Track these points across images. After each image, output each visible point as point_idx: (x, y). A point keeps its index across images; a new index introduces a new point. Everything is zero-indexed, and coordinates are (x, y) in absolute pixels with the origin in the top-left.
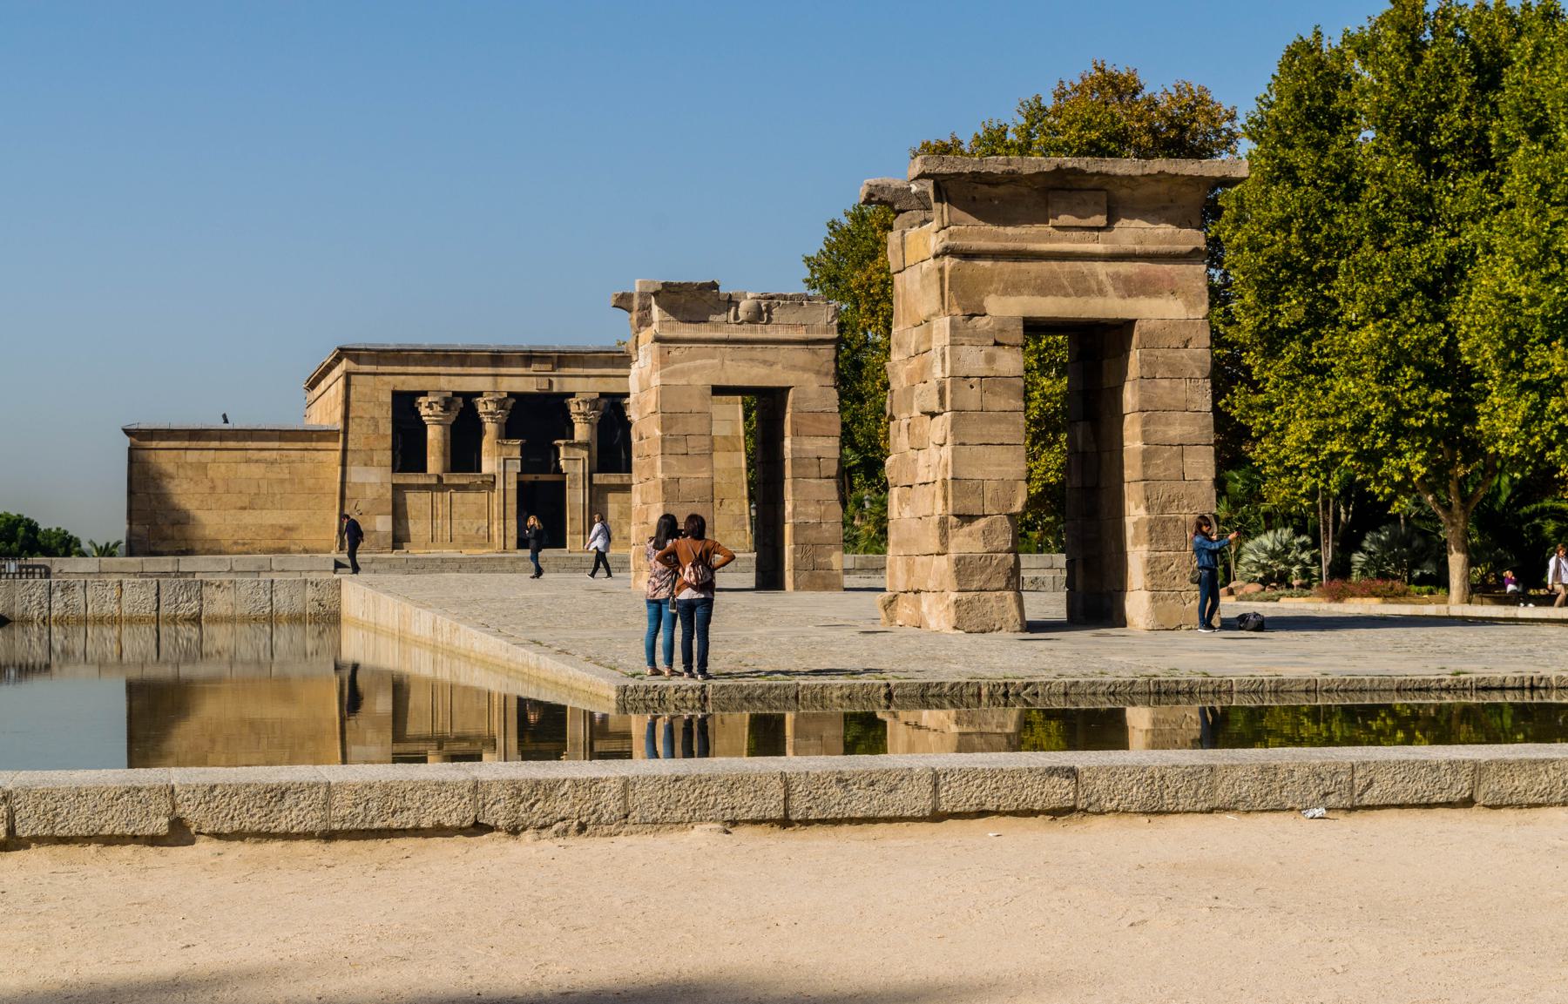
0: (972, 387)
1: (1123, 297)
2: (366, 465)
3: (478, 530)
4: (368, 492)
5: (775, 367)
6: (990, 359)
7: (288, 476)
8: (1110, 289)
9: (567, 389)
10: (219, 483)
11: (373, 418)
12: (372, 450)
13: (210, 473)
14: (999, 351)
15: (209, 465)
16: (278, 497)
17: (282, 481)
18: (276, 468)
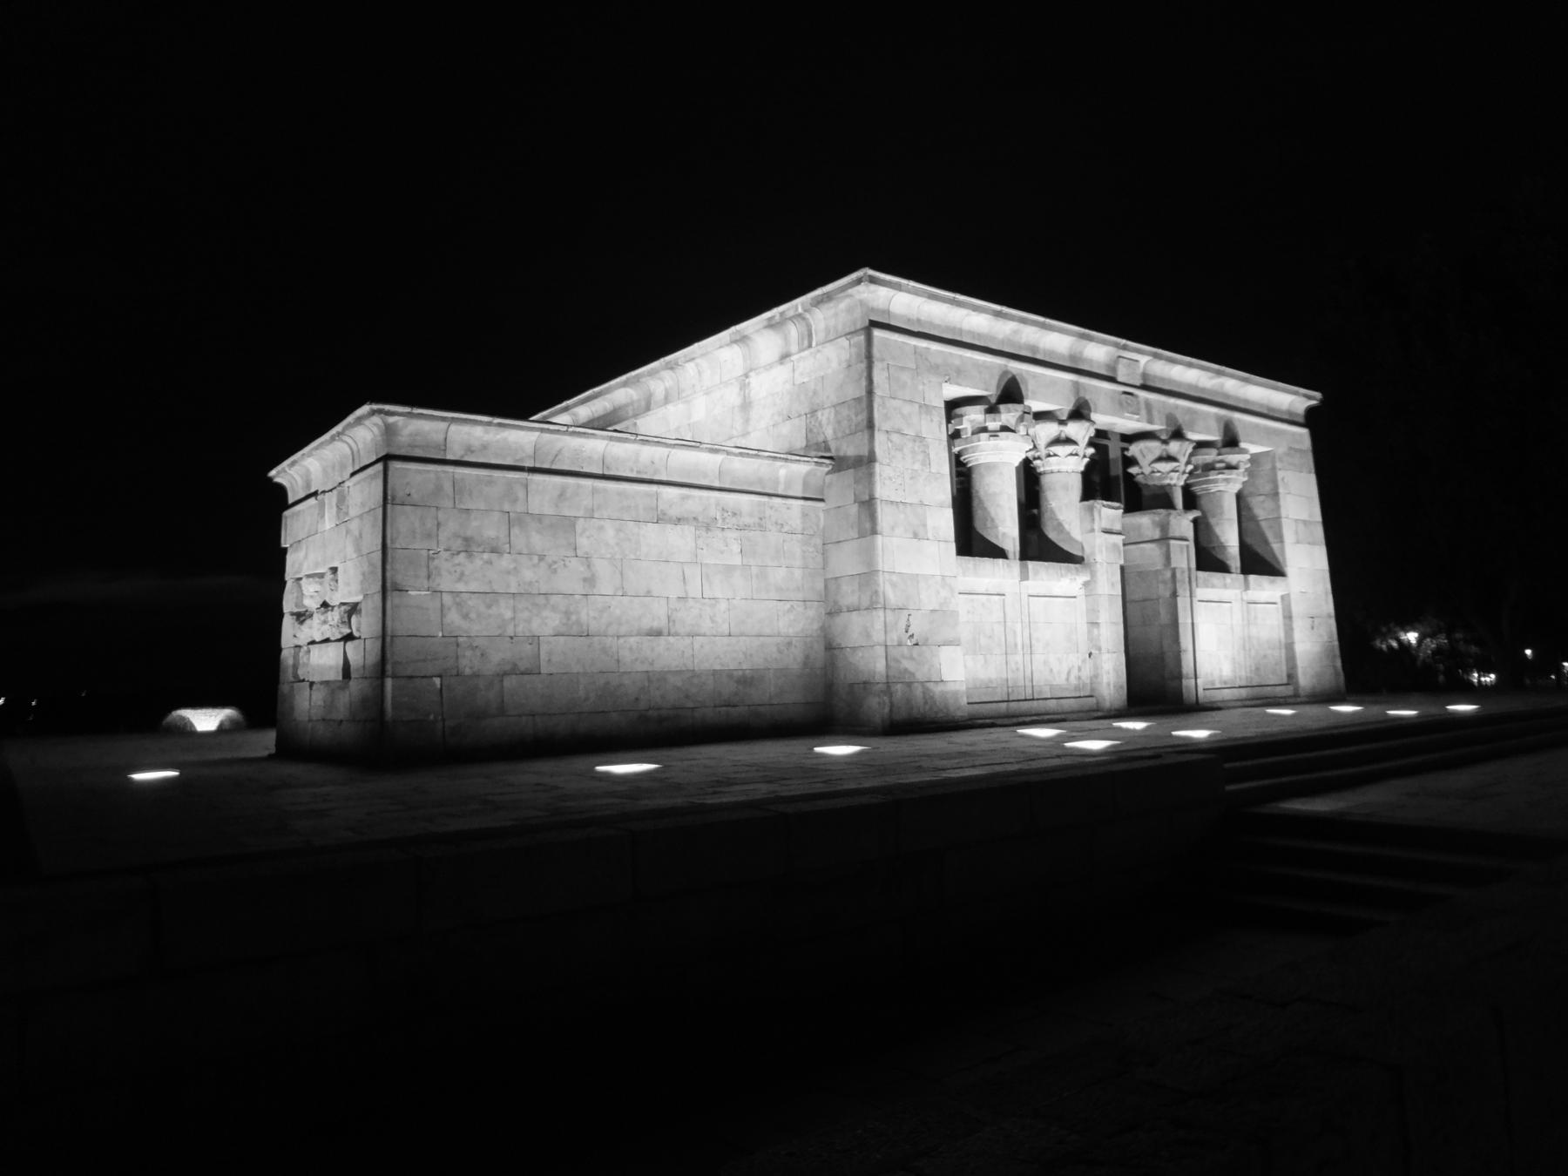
2: (916, 536)
7: (737, 560)
10: (602, 568)
11: (919, 438)
12: (922, 504)
13: (583, 543)
15: (580, 524)
16: (723, 606)
17: (729, 569)
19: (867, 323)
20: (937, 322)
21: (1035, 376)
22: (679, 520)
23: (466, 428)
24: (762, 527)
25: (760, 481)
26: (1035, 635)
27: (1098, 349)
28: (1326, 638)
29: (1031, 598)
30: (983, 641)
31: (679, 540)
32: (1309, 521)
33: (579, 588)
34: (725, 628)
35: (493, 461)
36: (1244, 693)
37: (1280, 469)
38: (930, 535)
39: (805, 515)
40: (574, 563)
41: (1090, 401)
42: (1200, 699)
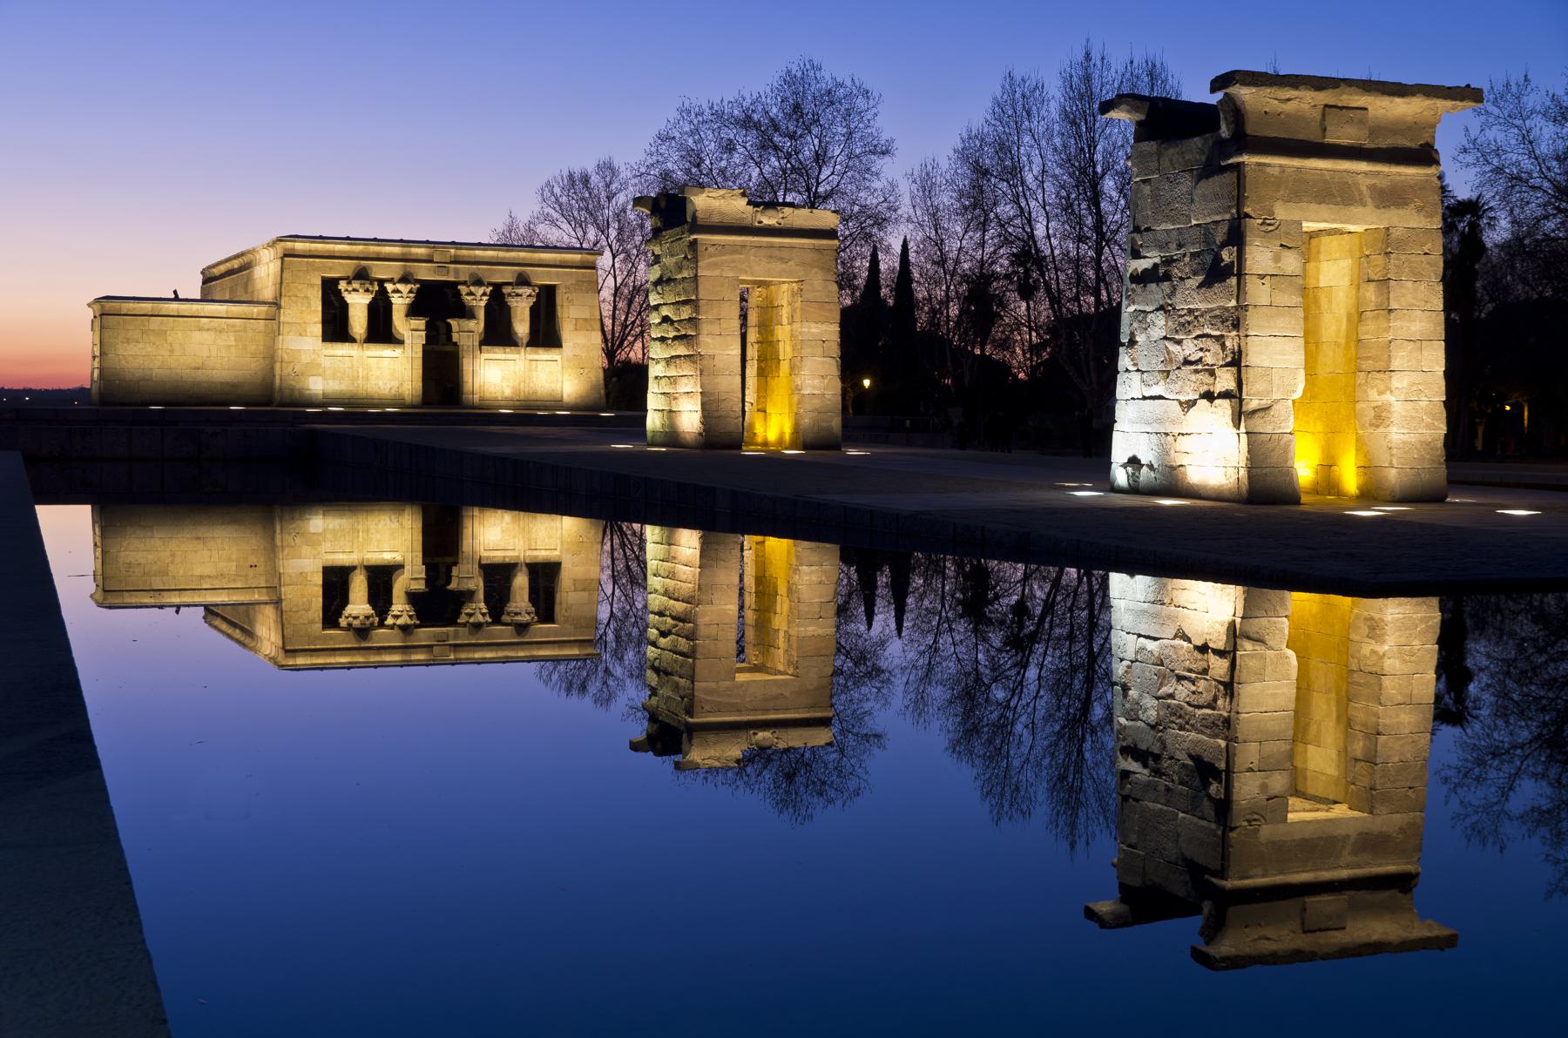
0: (1263, 284)
1: (1377, 207)
2: (300, 335)
3: (391, 389)
4: (303, 357)
5: (789, 264)
6: (1277, 259)
8: (1369, 200)
9: (462, 279)
10: (176, 346)
11: (306, 297)
12: (305, 323)
13: (170, 339)
14: (1286, 253)
15: (168, 332)
17: (229, 347)
18: (224, 336)
19: (282, 255)
21: (377, 265)
22: (208, 330)
23: (127, 304)
24: (245, 331)
25: (245, 314)
28: (594, 379)
31: (207, 337)
33: (167, 353)
34: (227, 367)
36: (518, 403)
39: (266, 326)
40: (166, 345)
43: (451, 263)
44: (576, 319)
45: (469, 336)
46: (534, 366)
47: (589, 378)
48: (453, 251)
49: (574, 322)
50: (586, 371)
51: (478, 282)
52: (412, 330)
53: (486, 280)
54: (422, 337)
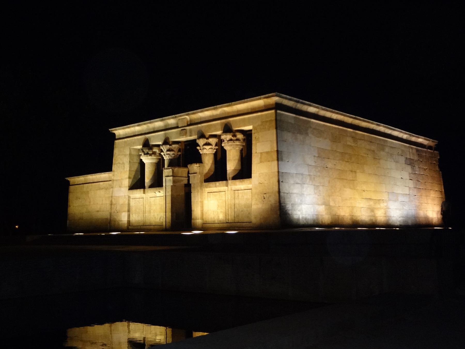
2: (120, 187)
3: (160, 218)
11: (123, 163)
13: (90, 195)
15: (89, 192)
20: (130, 132)
21: (153, 136)
26: (151, 208)
27: (171, 121)
29: (151, 198)
30: (138, 210)
32: (271, 151)
35: (80, 183)
37: (254, 133)
38: (123, 187)
41: (169, 137)
42: (167, 228)
43: (188, 125)
44: (261, 153)
45: (194, 177)
46: (237, 195)
47: (270, 201)
48: (187, 117)
49: (260, 155)
50: (268, 196)
51: (202, 136)
52: (166, 177)
53: (207, 134)
54: (170, 180)
